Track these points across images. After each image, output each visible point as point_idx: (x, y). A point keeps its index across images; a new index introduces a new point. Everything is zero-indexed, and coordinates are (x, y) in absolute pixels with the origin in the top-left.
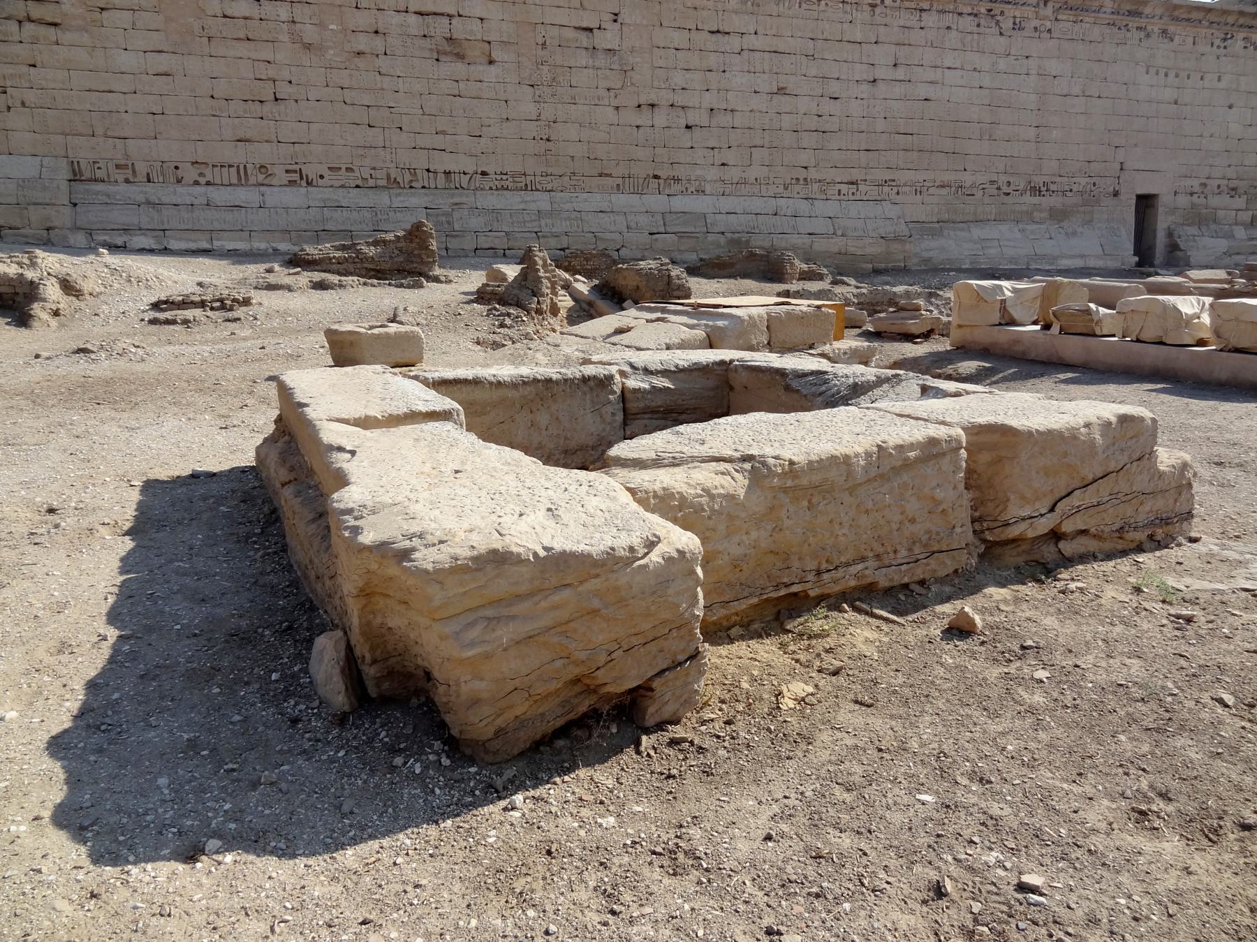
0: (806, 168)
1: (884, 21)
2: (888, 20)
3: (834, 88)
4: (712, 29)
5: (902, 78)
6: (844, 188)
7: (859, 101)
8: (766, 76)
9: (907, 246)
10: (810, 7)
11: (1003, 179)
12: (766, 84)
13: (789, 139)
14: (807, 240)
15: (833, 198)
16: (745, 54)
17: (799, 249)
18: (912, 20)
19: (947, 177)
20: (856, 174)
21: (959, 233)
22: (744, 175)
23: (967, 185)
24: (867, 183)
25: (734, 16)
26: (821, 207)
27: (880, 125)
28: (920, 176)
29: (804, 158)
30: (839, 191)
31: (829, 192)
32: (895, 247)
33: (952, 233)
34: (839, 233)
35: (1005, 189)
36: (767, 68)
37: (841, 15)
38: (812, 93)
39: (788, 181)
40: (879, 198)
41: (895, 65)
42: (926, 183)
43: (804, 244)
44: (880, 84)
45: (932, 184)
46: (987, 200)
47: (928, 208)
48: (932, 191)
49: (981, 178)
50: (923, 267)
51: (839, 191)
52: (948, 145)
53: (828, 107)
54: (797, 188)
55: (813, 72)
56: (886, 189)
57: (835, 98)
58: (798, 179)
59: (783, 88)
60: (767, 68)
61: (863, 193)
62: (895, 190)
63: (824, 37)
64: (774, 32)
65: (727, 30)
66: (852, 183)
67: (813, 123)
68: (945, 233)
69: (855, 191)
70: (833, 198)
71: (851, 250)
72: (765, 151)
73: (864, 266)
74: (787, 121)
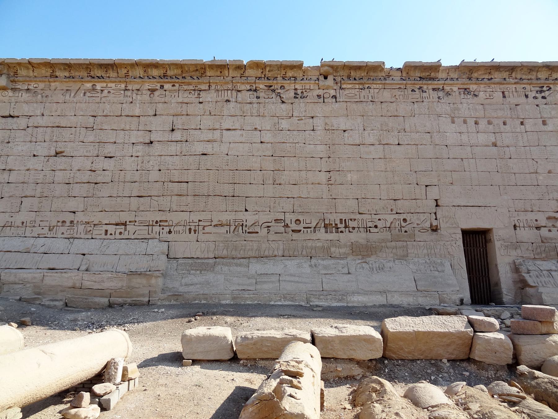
0: (74, 213)
1: (163, 100)
2: (166, 99)
3: (110, 149)
4: (4, 115)
5: (179, 139)
6: (111, 229)
7: (133, 158)
8: (46, 144)
9: (153, 281)
10: (94, 95)
11: (290, 218)
12: (42, 150)
13: (60, 190)
14: (38, 275)
15: (98, 237)
16: (30, 130)
17: (29, 283)
18: (192, 98)
19: (225, 217)
20: (124, 217)
21: (234, 269)
22: (11, 220)
23: (249, 224)
24: (136, 224)
25: (24, 105)
26: (80, 246)
27: (154, 175)
28: (195, 217)
29: (72, 204)
30: (106, 231)
31: (95, 232)
32: (137, 281)
33: (225, 269)
34: (83, 268)
35: (294, 226)
36: (47, 138)
37: (122, 98)
38: (86, 154)
39: (54, 223)
40: (148, 237)
41: (173, 130)
42: (201, 223)
43: (35, 278)
44: (155, 145)
45: (210, 224)
46: (272, 237)
47: (203, 245)
48: (207, 229)
49: (263, 218)
50: (173, 302)
51: (106, 231)
52: (227, 190)
53: (102, 163)
54: (63, 229)
55: (91, 139)
56: (157, 229)
57: (111, 157)
58: (64, 222)
59: (61, 152)
60: (47, 138)
61: (131, 233)
62: (167, 229)
63: (105, 114)
64: (59, 113)
65: (16, 114)
66: (123, 224)
67: (86, 176)
68: (218, 268)
69: (122, 231)
70: (98, 237)
71: (87, 284)
72: (36, 200)
73: (97, 300)
74: (60, 176)
